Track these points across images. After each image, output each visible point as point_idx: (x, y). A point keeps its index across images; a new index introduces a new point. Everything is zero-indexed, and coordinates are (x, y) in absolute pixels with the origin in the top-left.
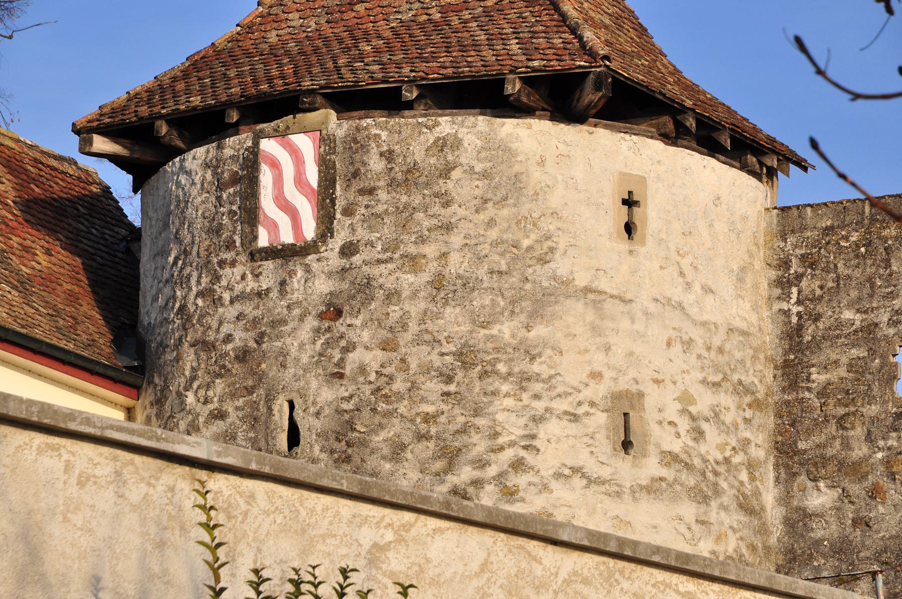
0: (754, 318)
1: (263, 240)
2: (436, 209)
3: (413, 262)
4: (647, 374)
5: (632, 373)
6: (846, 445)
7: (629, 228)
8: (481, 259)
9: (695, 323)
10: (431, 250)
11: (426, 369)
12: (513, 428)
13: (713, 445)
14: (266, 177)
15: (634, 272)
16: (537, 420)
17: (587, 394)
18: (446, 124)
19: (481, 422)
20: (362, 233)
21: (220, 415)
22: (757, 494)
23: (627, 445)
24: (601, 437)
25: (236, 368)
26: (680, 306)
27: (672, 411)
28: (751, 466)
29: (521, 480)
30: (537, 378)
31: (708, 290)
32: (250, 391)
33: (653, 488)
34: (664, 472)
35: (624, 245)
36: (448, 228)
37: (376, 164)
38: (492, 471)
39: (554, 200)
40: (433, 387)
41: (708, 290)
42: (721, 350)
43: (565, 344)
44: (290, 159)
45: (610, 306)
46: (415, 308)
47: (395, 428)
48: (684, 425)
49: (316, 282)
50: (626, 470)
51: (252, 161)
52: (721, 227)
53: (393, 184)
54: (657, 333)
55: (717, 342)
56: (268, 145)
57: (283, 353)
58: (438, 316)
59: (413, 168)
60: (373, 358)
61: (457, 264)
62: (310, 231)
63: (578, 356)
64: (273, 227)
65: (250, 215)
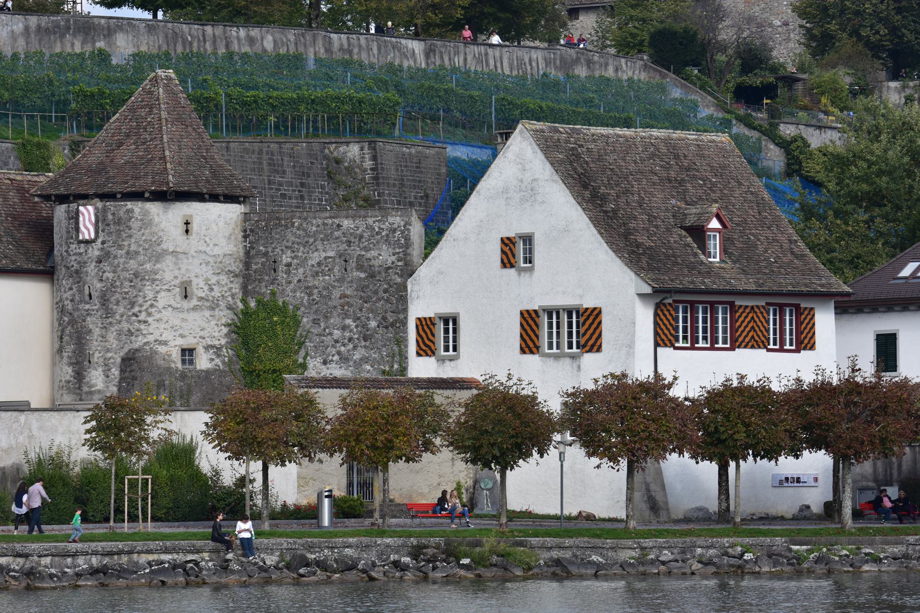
0: (235, 249)
1: (81, 238)
2: (127, 231)
3: (120, 247)
4: (193, 275)
5: (188, 275)
6: (260, 288)
7: (187, 231)
8: (141, 245)
9: (210, 256)
10: (125, 243)
11: (125, 279)
12: (150, 295)
13: (216, 293)
14: (81, 219)
15: (189, 244)
16: (157, 292)
17: (173, 283)
18: (129, 205)
19: (141, 294)
20: (107, 238)
21: (71, 289)
22: (235, 303)
23: (186, 297)
24: (178, 295)
25: (75, 275)
26: (205, 252)
27: (202, 284)
28: (233, 296)
29: (153, 310)
30: (157, 280)
31: (215, 245)
32: (79, 282)
33: (195, 309)
34: (198, 303)
35: (185, 237)
36: (130, 236)
37: (110, 217)
38: (144, 308)
39: (162, 226)
40: (127, 284)
41: (215, 245)
42: (221, 262)
43: (166, 269)
44: (87, 213)
45: (180, 256)
46: (122, 260)
47: (117, 295)
48: (206, 288)
49: (95, 251)
50: (186, 304)
51: (77, 212)
52: (221, 224)
53: (115, 223)
54: (197, 262)
55: (219, 260)
56: (81, 208)
57: (87, 272)
58: (128, 263)
59: (120, 219)
60: (110, 275)
61: (133, 247)
62: (93, 236)
63: (168, 271)
64: (83, 234)
65: (77, 229)
